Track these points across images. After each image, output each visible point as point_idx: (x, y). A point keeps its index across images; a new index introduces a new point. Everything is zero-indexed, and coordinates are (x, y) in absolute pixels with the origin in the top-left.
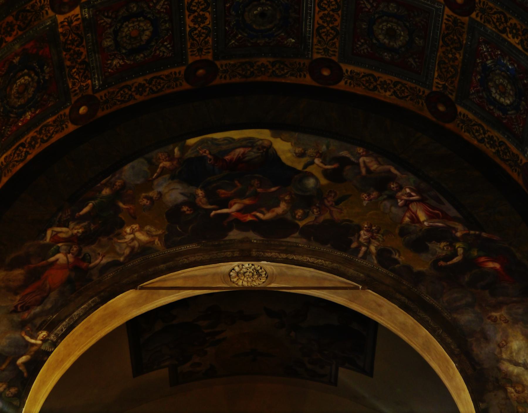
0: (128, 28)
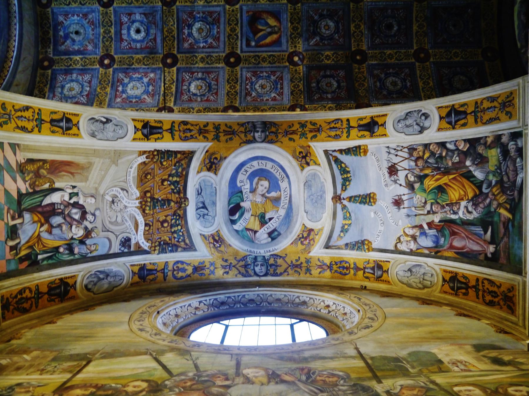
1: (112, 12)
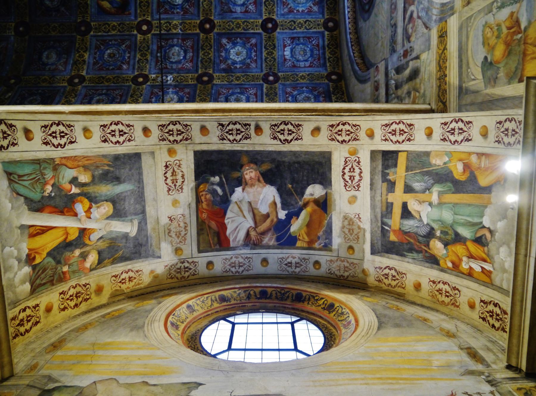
1: (264, 15)
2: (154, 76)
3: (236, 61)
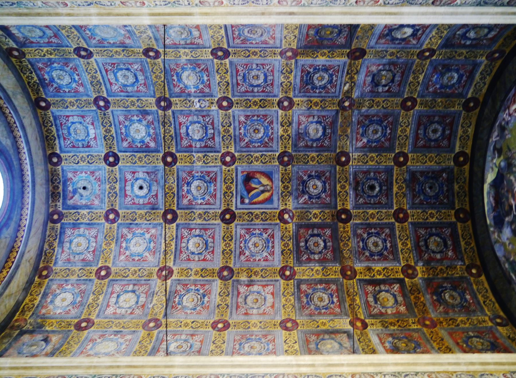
0: (432, 246)
1: (117, 170)
2: (213, 108)
3: (139, 123)
